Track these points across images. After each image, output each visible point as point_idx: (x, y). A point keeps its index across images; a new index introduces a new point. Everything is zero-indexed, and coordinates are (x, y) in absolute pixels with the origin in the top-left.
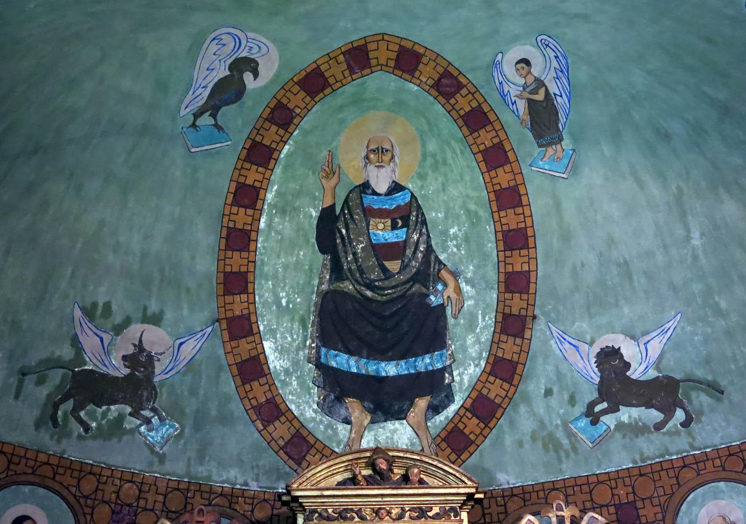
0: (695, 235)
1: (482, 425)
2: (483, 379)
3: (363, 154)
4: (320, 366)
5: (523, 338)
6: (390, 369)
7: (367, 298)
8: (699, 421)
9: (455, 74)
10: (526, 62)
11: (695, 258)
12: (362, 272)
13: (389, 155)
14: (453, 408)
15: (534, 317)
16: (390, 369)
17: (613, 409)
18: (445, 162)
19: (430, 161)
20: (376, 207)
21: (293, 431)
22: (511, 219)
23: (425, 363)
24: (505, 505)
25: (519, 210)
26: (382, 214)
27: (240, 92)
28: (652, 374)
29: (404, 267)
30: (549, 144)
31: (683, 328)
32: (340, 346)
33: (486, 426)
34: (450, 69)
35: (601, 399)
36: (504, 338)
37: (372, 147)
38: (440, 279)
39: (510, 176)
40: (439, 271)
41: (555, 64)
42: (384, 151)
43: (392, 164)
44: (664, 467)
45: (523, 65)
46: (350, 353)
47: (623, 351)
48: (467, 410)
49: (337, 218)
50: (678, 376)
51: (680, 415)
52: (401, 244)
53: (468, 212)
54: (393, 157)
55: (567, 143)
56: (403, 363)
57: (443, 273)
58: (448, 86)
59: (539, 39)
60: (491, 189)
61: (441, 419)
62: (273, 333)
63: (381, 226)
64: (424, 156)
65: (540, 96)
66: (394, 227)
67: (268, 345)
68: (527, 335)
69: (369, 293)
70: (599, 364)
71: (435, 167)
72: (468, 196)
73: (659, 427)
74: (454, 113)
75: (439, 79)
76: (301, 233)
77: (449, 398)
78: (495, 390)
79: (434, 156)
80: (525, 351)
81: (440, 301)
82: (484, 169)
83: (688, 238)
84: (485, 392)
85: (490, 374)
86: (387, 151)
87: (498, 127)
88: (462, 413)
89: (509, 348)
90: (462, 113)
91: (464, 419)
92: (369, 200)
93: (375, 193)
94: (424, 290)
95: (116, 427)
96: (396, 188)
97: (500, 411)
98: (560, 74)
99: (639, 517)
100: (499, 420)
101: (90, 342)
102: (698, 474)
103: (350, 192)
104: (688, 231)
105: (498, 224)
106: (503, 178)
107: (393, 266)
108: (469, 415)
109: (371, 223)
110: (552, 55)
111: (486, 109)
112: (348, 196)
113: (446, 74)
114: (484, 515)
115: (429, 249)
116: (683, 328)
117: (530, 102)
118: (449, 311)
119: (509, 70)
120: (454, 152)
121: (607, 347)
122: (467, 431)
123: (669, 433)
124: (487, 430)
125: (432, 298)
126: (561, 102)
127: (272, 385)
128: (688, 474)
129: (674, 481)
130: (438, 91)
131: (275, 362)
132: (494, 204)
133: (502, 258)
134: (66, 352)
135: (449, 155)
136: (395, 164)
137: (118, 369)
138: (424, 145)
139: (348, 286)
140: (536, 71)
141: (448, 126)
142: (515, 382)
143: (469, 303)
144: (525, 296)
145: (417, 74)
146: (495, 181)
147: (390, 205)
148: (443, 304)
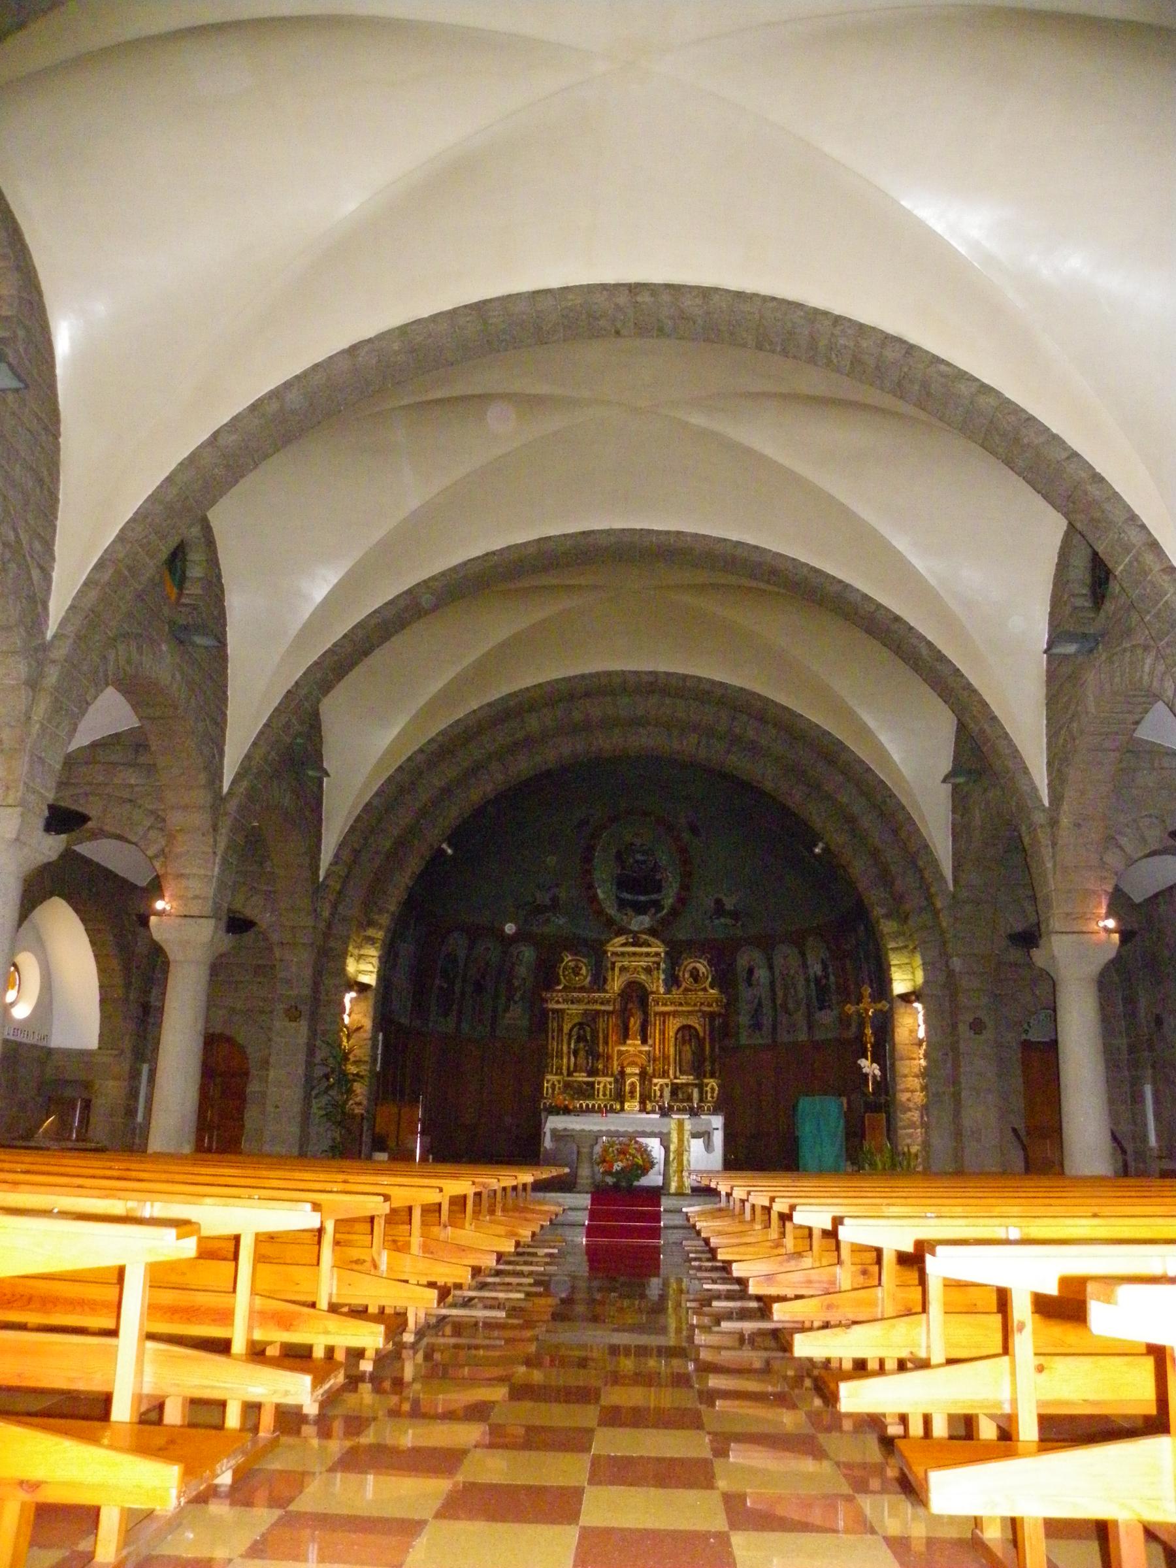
4: (617, 897)
6: (642, 898)
14: (665, 911)
16: (642, 898)
23: (654, 897)
27: (588, 822)
51: (740, 923)
61: (659, 915)
62: (599, 887)
67: (599, 891)
73: (734, 925)
77: (663, 909)
95: (548, 920)
96: (642, 845)
101: (538, 895)
107: (643, 867)
115: (656, 862)
127: (599, 904)
131: (601, 896)
134: (531, 900)
137: (548, 902)
143: (670, 879)
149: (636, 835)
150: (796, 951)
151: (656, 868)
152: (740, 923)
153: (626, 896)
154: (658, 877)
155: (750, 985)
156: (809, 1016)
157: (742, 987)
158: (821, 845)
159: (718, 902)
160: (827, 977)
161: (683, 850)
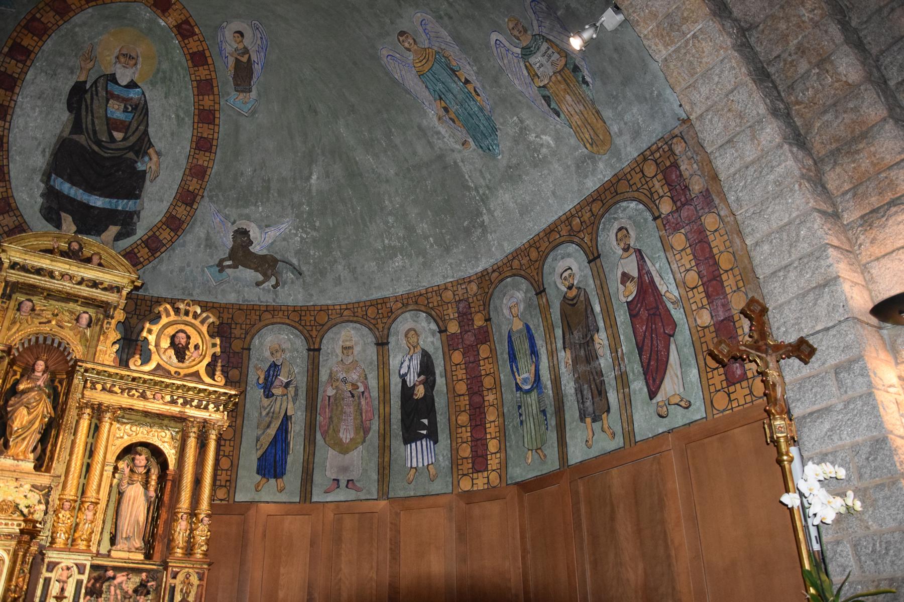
0: (314, 177)
1: (150, 254)
2: (159, 226)
3: (115, 55)
5: (192, 207)
6: (98, 202)
7: (94, 151)
8: (283, 287)
9: (193, 24)
10: (241, 34)
11: (310, 190)
12: (95, 132)
13: (134, 61)
15: (203, 197)
16: (98, 202)
17: (235, 266)
18: (171, 80)
19: (160, 75)
20: (116, 93)
21: (16, 223)
22: (205, 131)
23: (121, 205)
24: (151, 307)
25: (211, 126)
26: (117, 98)
28: (265, 252)
29: (124, 139)
30: (242, 91)
31: (290, 230)
32: (66, 177)
33: (153, 255)
34: (190, 20)
35: (230, 258)
36: (179, 204)
37: (124, 52)
38: (146, 153)
39: (212, 103)
40: (149, 148)
41: (259, 42)
42: (131, 58)
43: (134, 68)
44: (252, 308)
45: (238, 35)
46: (73, 184)
47: (251, 233)
48: (143, 242)
49: (86, 91)
50: (279, 257)
51: (273, 281)
52: (127, 123)
53: (178, 116)
54: (135, 64)
55: (254, 94)
56: (107, 200)
57: (151, 151)
58: (185, 30)
59: (253, 22)
60: (197, 107)
63: (116, 107)
64: (158, 70)
65: (244, 59)
66: (125, 110)
68: (195, 207)
69: (96, 148)
70: (234, 237)
71: (163, 80)
72: (180, 106)
73: (258, 284)
74: (185, 49)
75: (181, 23)
76: (57, 93)
78: (165, 235)
79: (164, 72)
80: (191, 215)
81: (144, 168)
82: (196, 93)
83: (309, 178)
84: (157, 233)
85: (164, 224)
86: (133, 58)
87: (212, 69)
88: (138, 242)
89: (181, 211)
90: (191, 51)
91: (139, 247)
92: (111, 87)
93: (117, 83)
94: (136, 158)
96: (132, 85)
97: (164, 248)
98: (260, 49)
99: (231, 333)
100: (162, 253)
102: (273, 317)
103: (100, 77)
104: (311, 174)
105: (195, 131)
106: (207, 102)
107: (118, 136)
108: (143, 245)
109: (110, 102)
110: (259, 36)
111: (207, 54)
112: (98, 79)
113: (186, 22)
114: (136, 309)
115: (146, 133)
116: (290, 230)
117: (236, 58)
118: (148, 176)
119: (228, 34)
120: (179, 75)
121: (242, 228)
122: (139, 255)
123: (264, 289)
124: (152, 258)
125: (139, 164)
126: (257, 68)
128: (267, 316)
129: (258, 318)
130: (178, 31)
132: (196, 117)
133: (192, 154)
135: (175, 75)
136: (137, 69)
138: (159, 63)
139: (82, 139)
140: (247, 42)
141: (178, 55)
142: (179, 233)
144: (200, 182)
145: (167, 14)
146: (201, 103)
147: (124, 93)
148: (145, 171)
149: (127, 58)
150: (371, 339)
151: (142, 146)
152: (273, 281)
153: (66, 188)
154: (140, 166)
155: (268, 395)
156: (384, 448)
157: (255, 394)
158: (588, 34)
159: (242, 233)
160: (430, 384)
161: (206, 117)
